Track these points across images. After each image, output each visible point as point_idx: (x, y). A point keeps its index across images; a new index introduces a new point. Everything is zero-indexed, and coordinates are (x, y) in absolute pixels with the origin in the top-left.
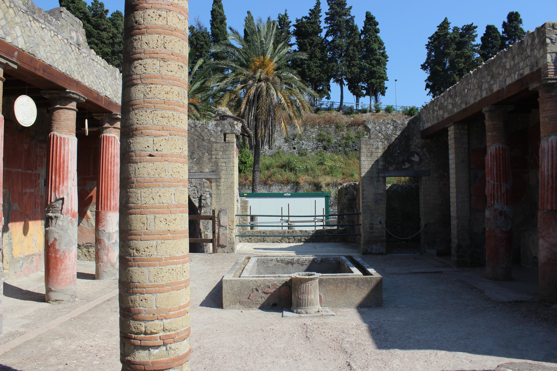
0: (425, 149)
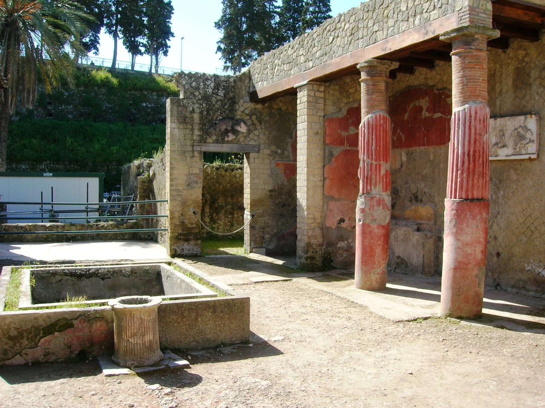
0: (254, 117)
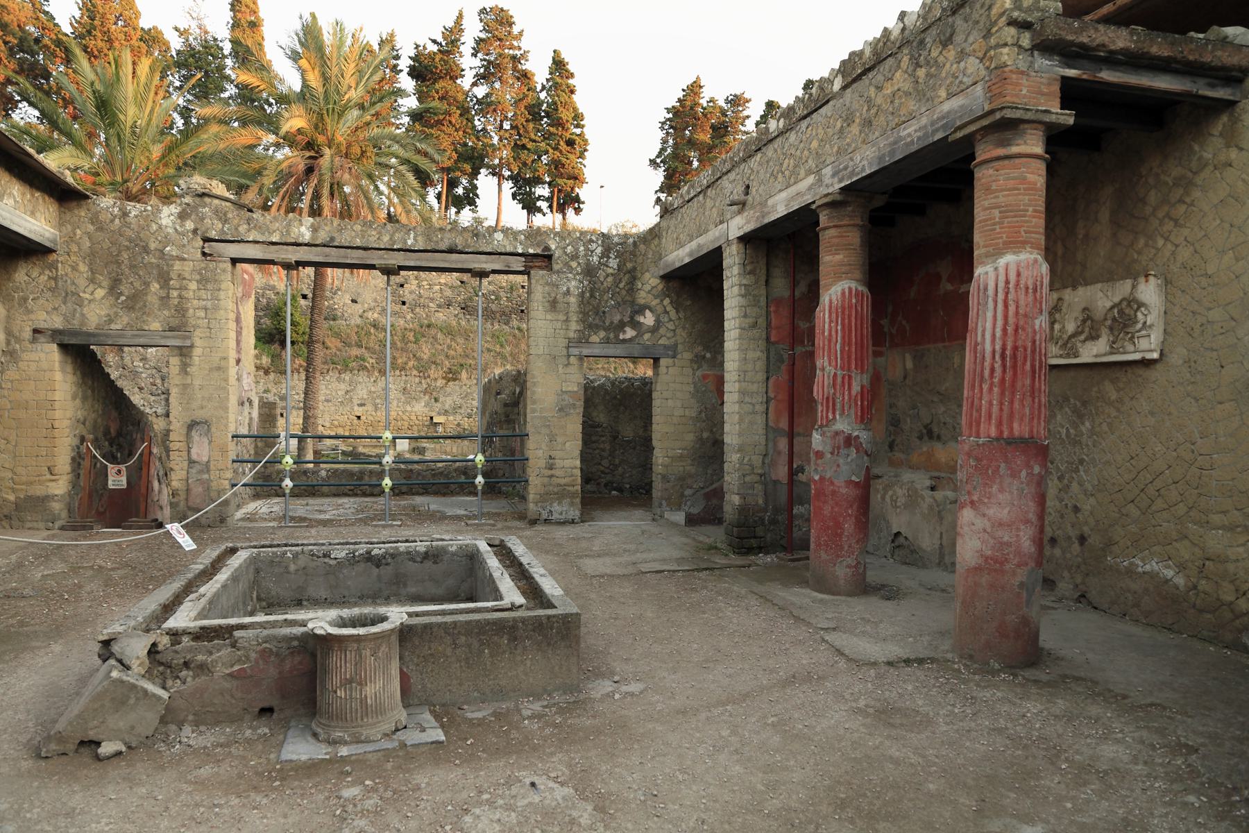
0: (667, 301)
